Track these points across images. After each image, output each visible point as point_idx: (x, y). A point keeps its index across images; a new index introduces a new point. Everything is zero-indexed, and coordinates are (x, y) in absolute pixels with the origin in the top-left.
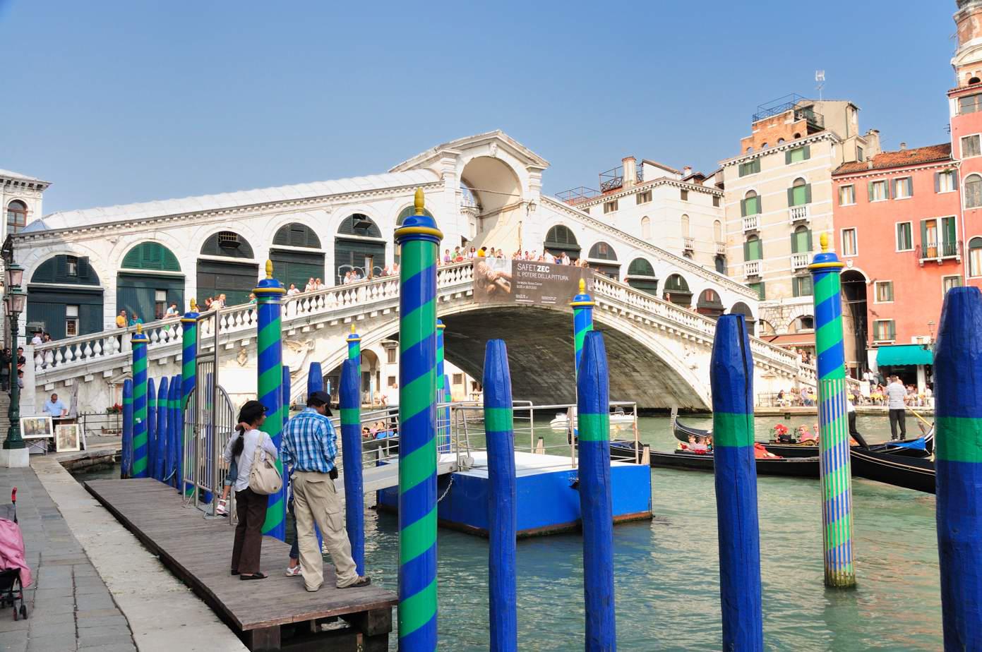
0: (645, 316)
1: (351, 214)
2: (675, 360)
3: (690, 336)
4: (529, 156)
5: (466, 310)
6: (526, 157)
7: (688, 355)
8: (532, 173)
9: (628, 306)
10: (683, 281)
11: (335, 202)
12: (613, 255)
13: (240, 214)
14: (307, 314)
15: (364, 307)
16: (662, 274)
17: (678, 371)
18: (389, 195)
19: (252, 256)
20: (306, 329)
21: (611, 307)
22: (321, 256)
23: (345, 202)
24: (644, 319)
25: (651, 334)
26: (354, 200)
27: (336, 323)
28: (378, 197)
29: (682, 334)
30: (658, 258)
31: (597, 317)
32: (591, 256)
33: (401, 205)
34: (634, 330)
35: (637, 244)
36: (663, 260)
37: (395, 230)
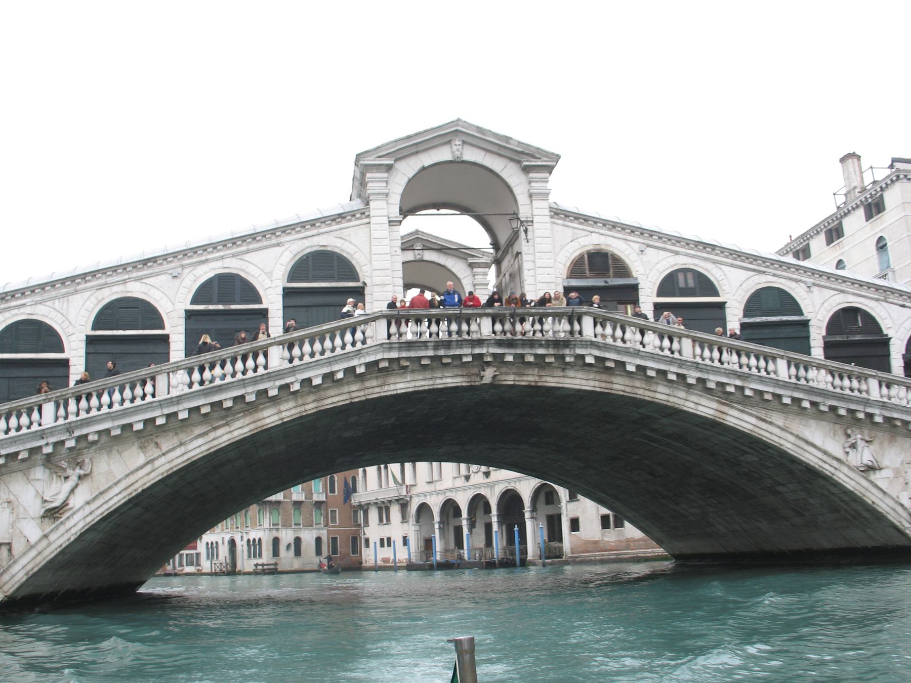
0: (739, 383)
1: (211, 275)
2: (825, 458)
3: (851, 412)
4: (519, 149)
5: (364, 398)
6: (516, 151)
8: (531, 175)
9: (697, 366)
10: (870, 319)
11: (187, 261)
13: (46, 296)
14: (72, 418)
15: (161, 404)
16: (818, 308)
17: (835, 477)
18: (274, 241)
19: (62, 350)
20: (71, 444)
21: (662, 373)
22: (165, 339)
23: (203, 258)
24: (741, 389)
27: (118, 432)
28: (255, 245)
29: (833, 409)
30: (805, 283)
31: (641, 392)
32: (659, 294)
33: (294, 253)
35: (759, 265)
37: (284, 289)
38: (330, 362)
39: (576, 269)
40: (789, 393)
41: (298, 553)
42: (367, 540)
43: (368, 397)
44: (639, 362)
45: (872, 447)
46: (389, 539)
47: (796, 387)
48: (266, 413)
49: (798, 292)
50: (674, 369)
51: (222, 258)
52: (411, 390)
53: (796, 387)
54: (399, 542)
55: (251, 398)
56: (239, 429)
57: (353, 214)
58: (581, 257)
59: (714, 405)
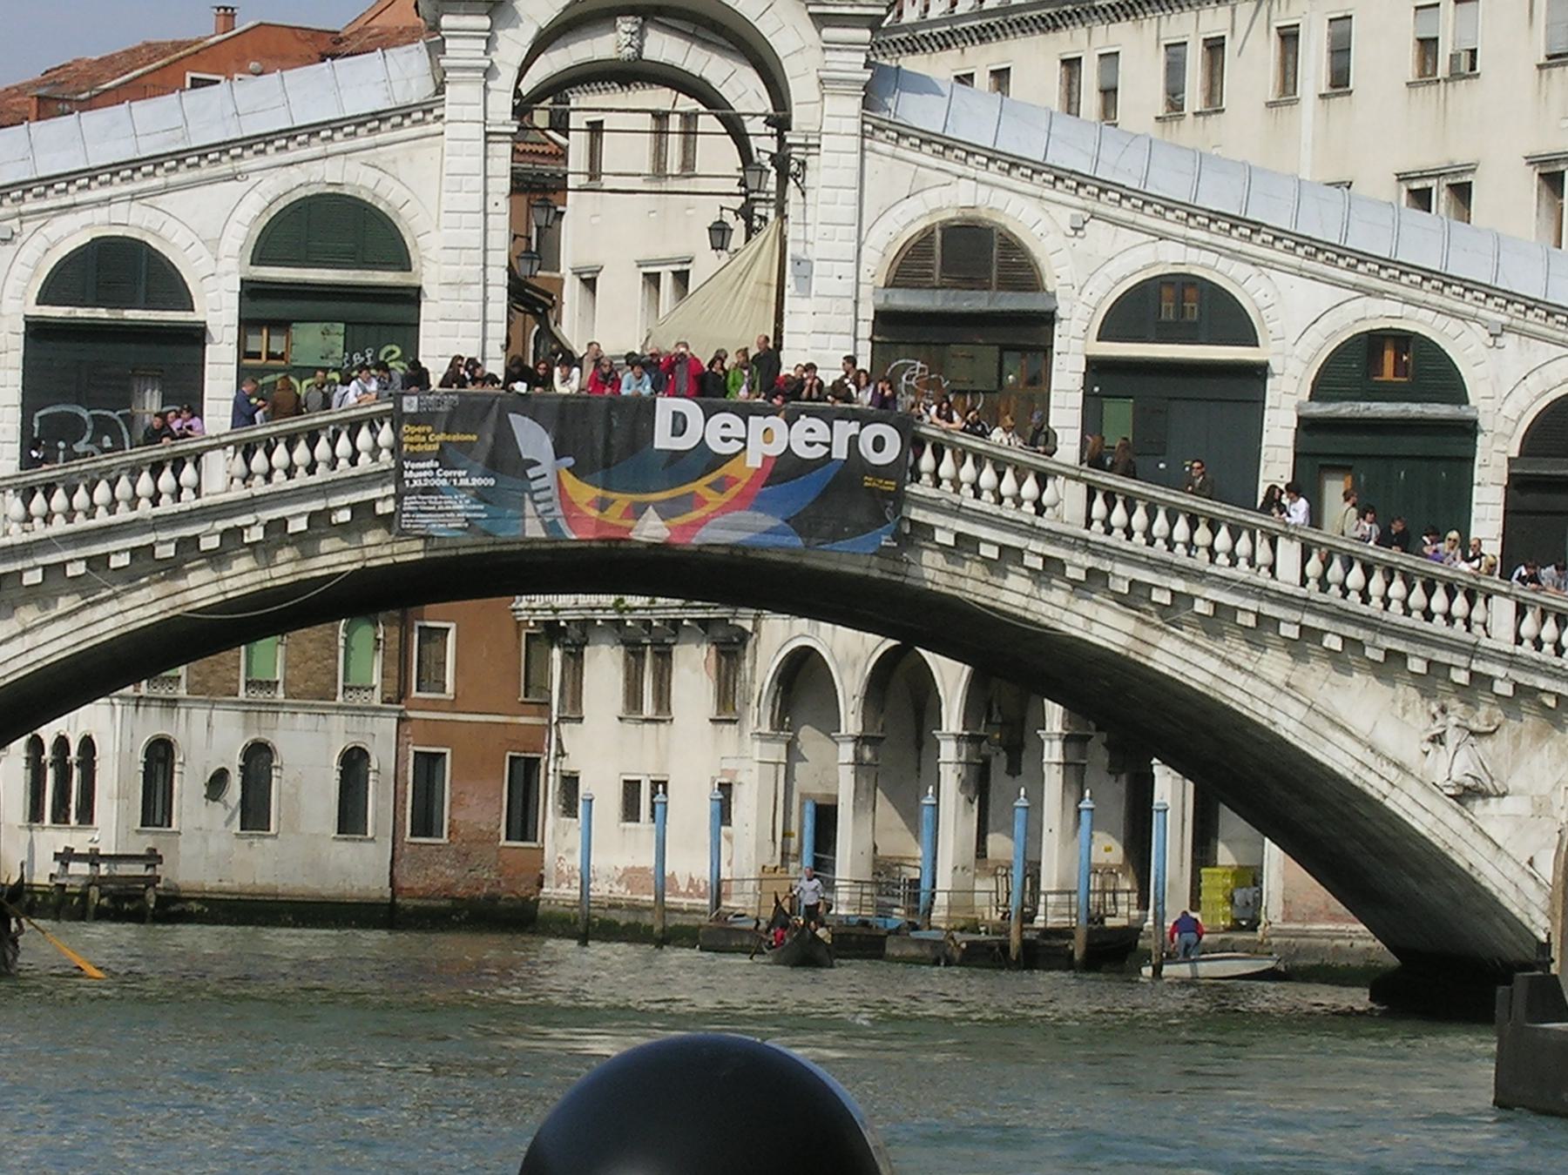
0: (1180, 585)
1: (84, 238)
2: (1369, 758)
7: (1437, 739)
11: (31, 204)
12: (1240, 328)
17: (1388, 803)
18: (226, 167)
21: (1011, 555)
25: (1240, 652)
26: (97, 193)
31: (970, 585)
33: (269, 198)
34: (1149, 634)
36: (1521, 333)
37: (242, 281)
38: (324, 490)
39: (911, 265)
40: (1296, 616)
41: (254, 814)
42: (570, 783)
43: (398, 559)
44: (962, 526)
45: (1488, 744)
46: (659, 786)
47: (1307, 605)
48: (193, 579)
49: (1464, 345)
50: (1035, 546)
51: (108, 201)
52: (486, 549)
53: (1307, 605)
54: (689, 807)
55: (168, 551)
56: (140, 608)
57: (405, 112)
58: (927, 235)
59: (1129, 625)
